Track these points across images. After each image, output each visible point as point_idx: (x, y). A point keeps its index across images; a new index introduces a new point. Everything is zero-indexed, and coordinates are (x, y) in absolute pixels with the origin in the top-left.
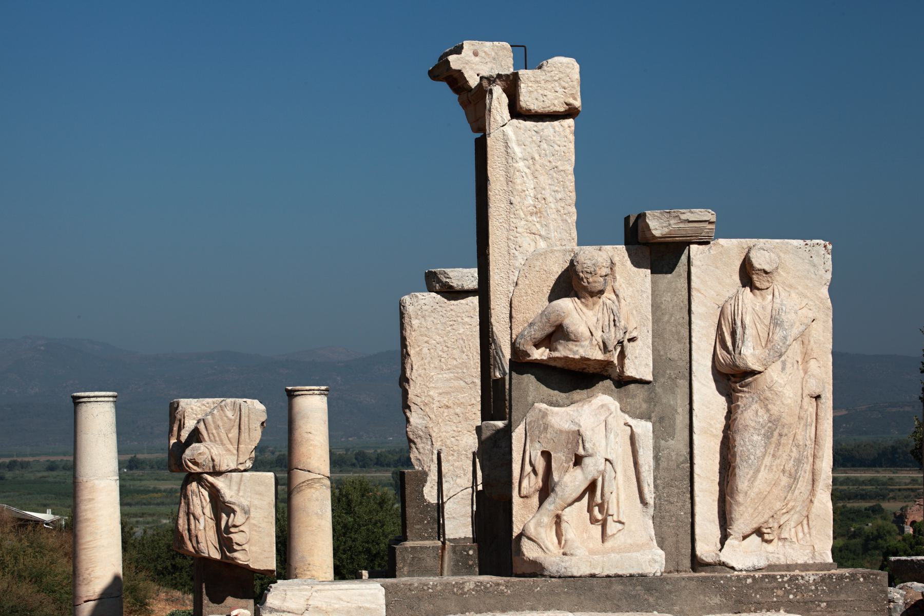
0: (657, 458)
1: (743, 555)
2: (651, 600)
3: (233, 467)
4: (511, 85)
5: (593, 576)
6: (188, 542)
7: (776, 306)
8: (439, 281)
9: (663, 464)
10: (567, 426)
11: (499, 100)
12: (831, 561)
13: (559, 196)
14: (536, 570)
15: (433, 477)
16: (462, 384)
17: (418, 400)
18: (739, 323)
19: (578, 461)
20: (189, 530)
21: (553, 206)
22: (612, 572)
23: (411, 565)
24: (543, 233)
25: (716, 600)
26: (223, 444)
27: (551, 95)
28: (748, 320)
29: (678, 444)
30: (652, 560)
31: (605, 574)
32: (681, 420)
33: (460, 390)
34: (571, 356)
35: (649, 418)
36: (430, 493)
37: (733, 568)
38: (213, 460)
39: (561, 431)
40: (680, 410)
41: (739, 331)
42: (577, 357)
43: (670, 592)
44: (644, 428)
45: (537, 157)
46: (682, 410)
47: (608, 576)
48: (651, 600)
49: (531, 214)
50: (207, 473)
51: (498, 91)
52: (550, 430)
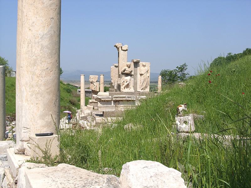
4: (121, 47)
15: (113, 83)
36: (113, 85)
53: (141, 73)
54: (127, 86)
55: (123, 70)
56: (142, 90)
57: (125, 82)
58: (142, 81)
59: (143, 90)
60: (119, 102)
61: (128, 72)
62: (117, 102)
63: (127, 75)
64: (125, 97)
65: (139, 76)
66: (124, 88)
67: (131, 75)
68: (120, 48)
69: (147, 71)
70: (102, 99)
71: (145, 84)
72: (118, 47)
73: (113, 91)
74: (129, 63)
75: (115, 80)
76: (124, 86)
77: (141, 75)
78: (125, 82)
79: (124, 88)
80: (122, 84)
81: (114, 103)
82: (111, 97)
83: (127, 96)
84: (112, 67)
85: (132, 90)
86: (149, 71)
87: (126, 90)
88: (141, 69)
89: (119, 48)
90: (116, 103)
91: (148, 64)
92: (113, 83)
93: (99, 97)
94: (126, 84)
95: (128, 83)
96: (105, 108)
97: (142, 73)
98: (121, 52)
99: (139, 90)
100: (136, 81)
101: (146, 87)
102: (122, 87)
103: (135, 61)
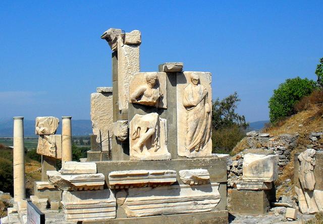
2: (168, 167)
4: (124, 38)
5: (152, 160)
9: (169, 131)
15: (99, 136)
19: (148, 129)
25: (184, 166)
33: (105, 116)
36: (98, 140)
53: (187, 103)
54: (149, 142)
55: (135, 93)
56: (192, 150)
57: (143, 129)
58: (192, 125)
59: (194, 152)
60: (126, 190)
61: (150, 100)
62: (120, 190)
63: (148, 108)
64: (147, 174)
65: (180, 110)
68: (120, 39)
69: (204, 98)
70: (77, 184)
71: (201, 135)
72: (113, 38)
73: (97, 157)
74: (151, 74)
75: (105, 128)
76: (140, 141)
77: (189, 107)
78: (143, 129)
79: (141, 148)
82: (102, 176)
83: (151, 172)
84: (93, 95)
86: (210, 98)
87: (147, 154)
88: (186, 93)
89: (116, 39)
90: (119, 193)
91: (205, 76)
93: (68, 178)
94: (144, 135)
95: (151, 131)
96: (84, 211)
97: (192, 101)
98: (123, 50)
99: (183, 151)
100: (172, 125)
101: (202, 144)
102: (134, 146)
103: (170, 67)
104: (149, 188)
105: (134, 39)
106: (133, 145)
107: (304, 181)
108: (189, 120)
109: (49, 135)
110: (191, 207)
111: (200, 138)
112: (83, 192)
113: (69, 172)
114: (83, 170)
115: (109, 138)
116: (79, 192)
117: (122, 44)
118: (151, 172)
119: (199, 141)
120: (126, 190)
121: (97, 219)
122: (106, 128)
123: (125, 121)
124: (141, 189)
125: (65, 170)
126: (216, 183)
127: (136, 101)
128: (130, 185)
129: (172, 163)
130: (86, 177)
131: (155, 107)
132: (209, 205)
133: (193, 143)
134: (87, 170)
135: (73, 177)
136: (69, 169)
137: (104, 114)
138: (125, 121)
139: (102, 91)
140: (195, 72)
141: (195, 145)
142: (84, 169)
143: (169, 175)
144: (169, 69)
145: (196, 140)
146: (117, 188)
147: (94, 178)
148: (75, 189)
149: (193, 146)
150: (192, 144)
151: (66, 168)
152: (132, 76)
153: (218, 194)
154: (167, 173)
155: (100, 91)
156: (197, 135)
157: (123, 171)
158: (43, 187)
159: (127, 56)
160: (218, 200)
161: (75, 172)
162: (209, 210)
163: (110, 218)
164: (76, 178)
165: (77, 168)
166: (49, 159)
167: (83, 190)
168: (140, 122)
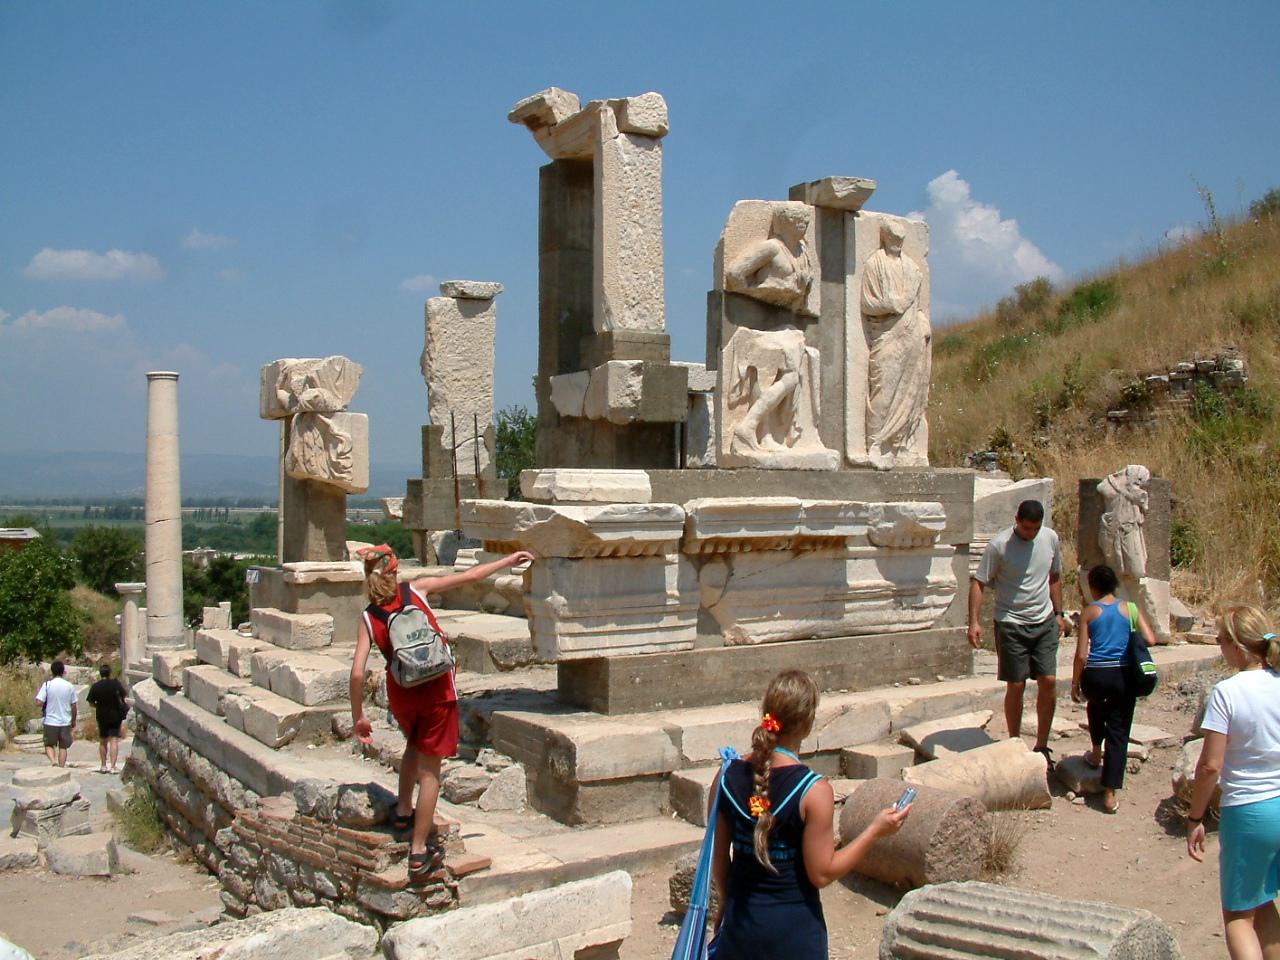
0: (822, 381)
1: (880, 459)
2: (834, 490)
3: (339, 407)
4: (620, 109)
5: (794, 469)
6: (302, 465)
7: (904, 265)
8: (456, 289)
9: (826, 384)
10: (771, 346)
11: (608, 116)
12: (928, 464)
13: (652, 196)
14: (747, 464)
15: (448, 429)
16: (468, 364)
17: (438, 374)
18: (884, 276)
19: (779, 375)
20: (304, 456)
21: (647, 202)
22: (808, 467)
23: (433, 492)
24: (641, 222)
25: (875, 491)
26: (331, 389)
27: (651, 119)
28: (889, 273)
29: (834, 370)
30: (831, 457)
31: (803, 468)
32: (837, 349)
33: (466, 368)
34: (778, 287)
35: (816, 347)
36: (446, 442)
37: (876, 468)
38: (325, 402)
39: (766, 350)
40: (836, 342)
41: (885, 281)
42: (783, 288)
43: (846, 484)
44: (814, 353)
45: (638, 164)
46: (838, 343)
47: (805, 470)
48: (834, 490)
49: (634, 207)
50: (322, 413)
51: (611, 112)
52: (756, 349)
60: (727, 557)
61: (790, 284)
62: (710, 558)
66: (760, 433)
67: (802, 320)
68: (608, 116)
76: (757, 408)
79: (760, 433)
80: (734, 397)
81: (692, 573)
83: (807, 503)
85: (808, 448)
92: (448, 429)
104: (787, 555)
105: (651, 119)
106: (730, 421)
107: (1120, 553)
108: (880, 356)
109: (330, 413)
110: (888, 615)
111: (907, 411)
112: (610, 562)
113: (574, 497)
114: (613, 491)
115: (476, 436)
116: (600, 563)
117: (615, 131)
118: (807, 503)
119: (904, 419)
120: (727, 557)
121: (645, 649)
122: (470, 405)
123: (636, 362)
124: (767, 557)
125: (564, 490)
126: (949, 546)
127: (746, 287)
128: (743, 543)
129: (846, 480)
130: (630, 511)
131: (789, 311)
132: (927, 610)
133: (890, 425)
134: (624, 492)
135: (594, 513)
136: (573, 486)
137: (464, 364)
138: (636, 362)
139: (463, 293)
140: (892, 216)
141: (894, 430)
142: (615, 486)
143: (851, 514)
144: (839, 195)
145: (894, 420)
146: (709, 550)
147: (656, 517)
148: (592, 552)
149: (889, 435)
150: (887, 428)
151: (565, 485)
152: (640, 231)
153: (953, 577)
154: (847, 508)
155: (454, 293)
156: (900, 402)
157: (720, 499)
158: (314, 577)
159: (627, 168)
160: (950, 598)
161: (589, 497)
162: (929, 624)
163: (681, 646)
164: (605, 513)
165: (596, 485)
166: (326, 490)
167: (613, 556)
168: (755, 352)
